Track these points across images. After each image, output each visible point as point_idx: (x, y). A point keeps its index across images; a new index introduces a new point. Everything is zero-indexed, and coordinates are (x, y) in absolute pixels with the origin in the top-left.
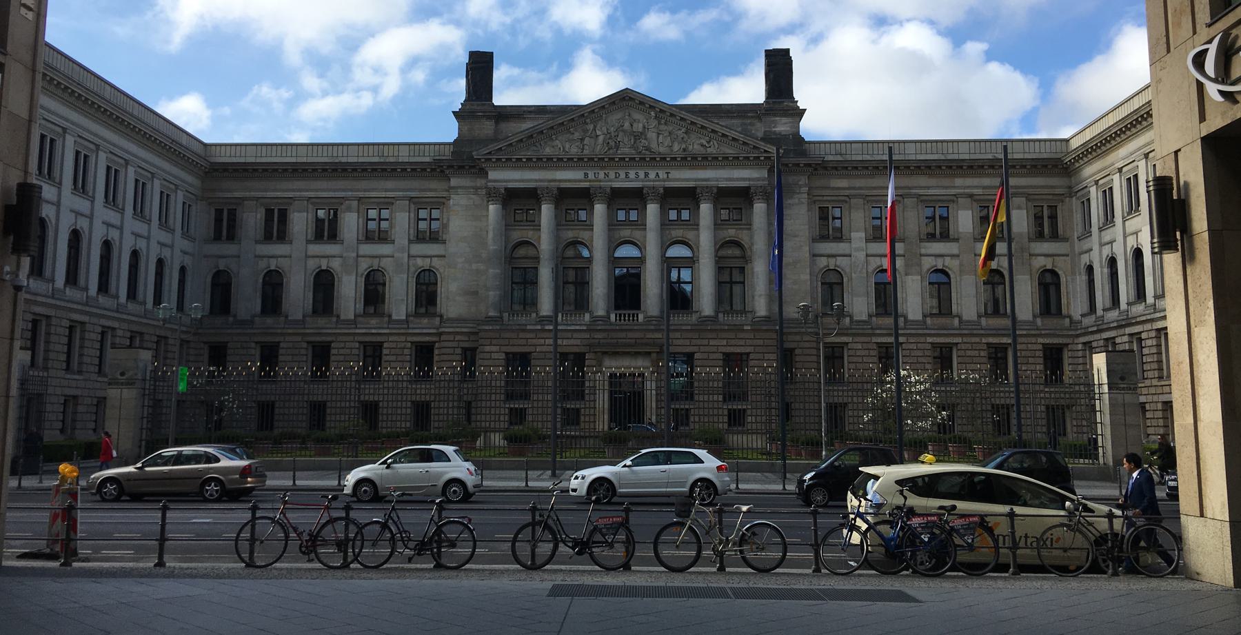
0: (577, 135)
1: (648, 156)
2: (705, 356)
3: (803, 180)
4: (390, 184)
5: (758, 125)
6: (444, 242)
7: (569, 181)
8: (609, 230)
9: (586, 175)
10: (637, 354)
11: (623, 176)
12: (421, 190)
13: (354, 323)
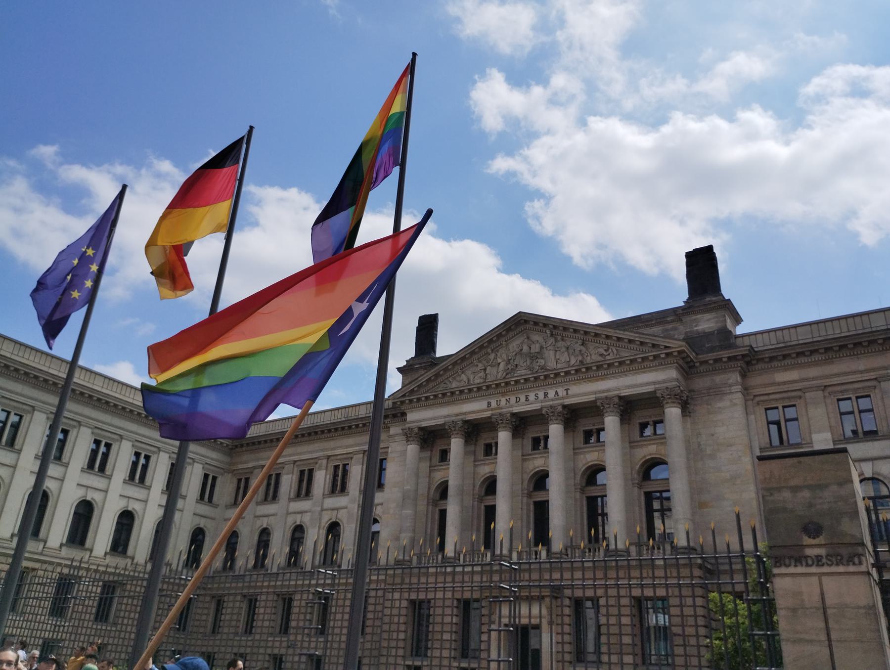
4: (350, 441)
7: (474, 412)
9: (489, 404)
11: (523, 399)
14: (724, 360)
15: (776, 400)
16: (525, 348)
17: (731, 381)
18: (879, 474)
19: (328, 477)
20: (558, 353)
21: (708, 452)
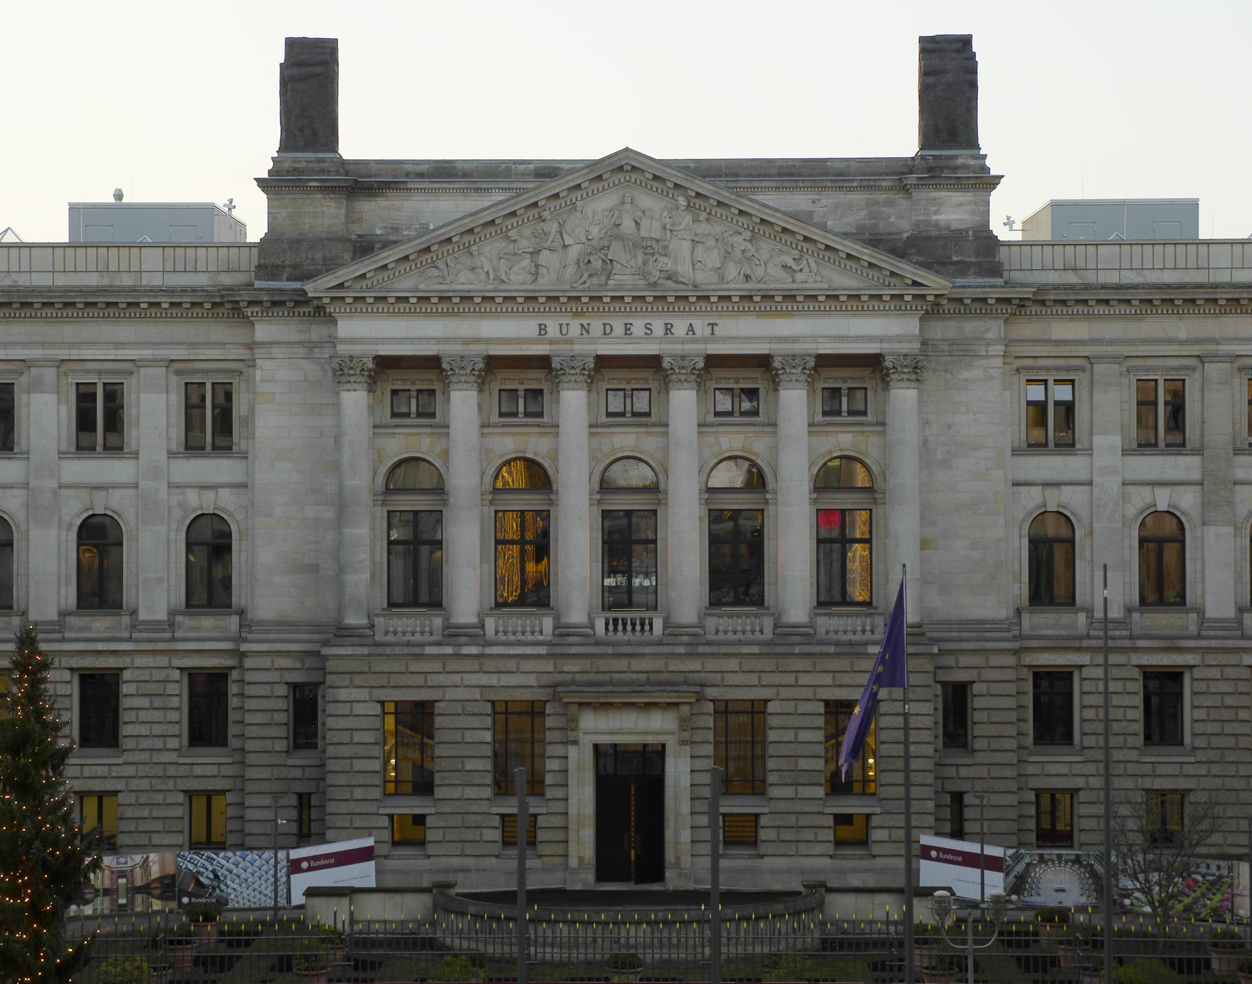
0: (525, 245)
1: (671, 289)
2: (789, 707)
3: (993, 328)
4: (124, 331)
5: (902, 203)
6: (244, 456)
7: (508, 341)
8: (591, 435)
9: (542, 328)
10: (649, 706)
11: (619, 330)
12: (193, 345)
14: (990, 301)
15: (1048, 369)
16: (627, 225)
17: (989, 335)
18: (1176, 508)
19: (64, 409)
20: (700, 248)
21: (940, 456)
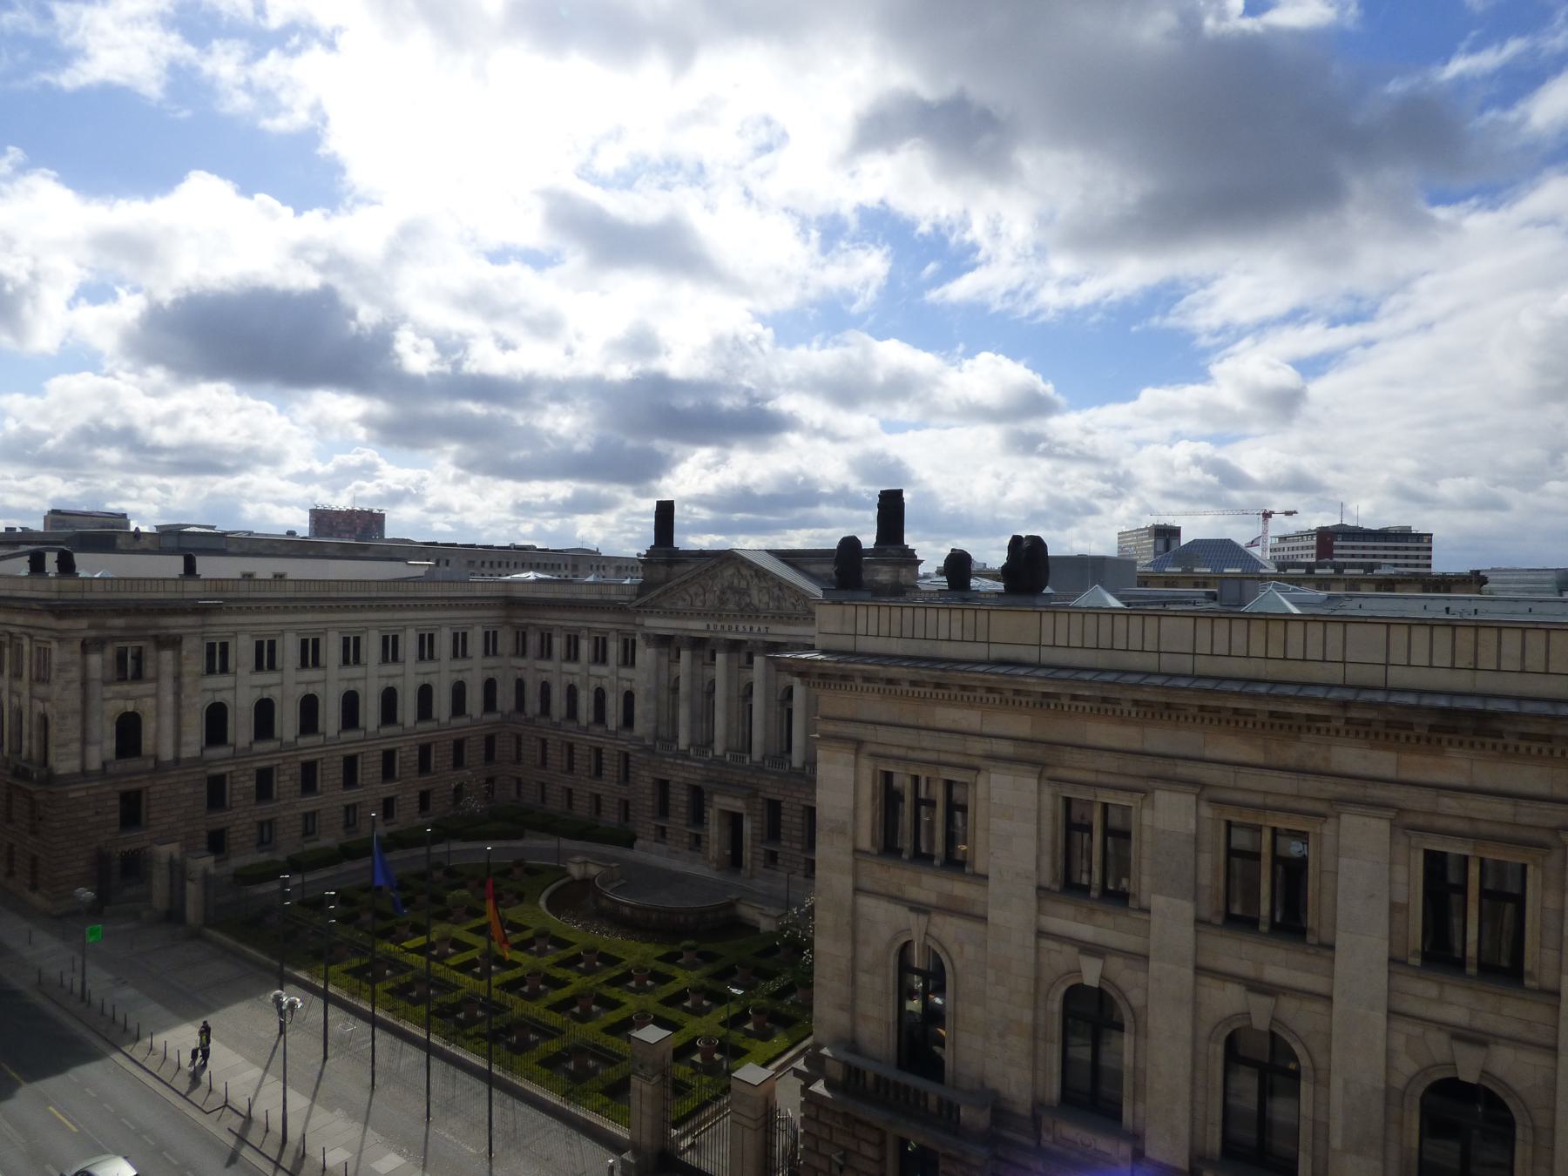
4: (606, 617)
13: (587, 729)
